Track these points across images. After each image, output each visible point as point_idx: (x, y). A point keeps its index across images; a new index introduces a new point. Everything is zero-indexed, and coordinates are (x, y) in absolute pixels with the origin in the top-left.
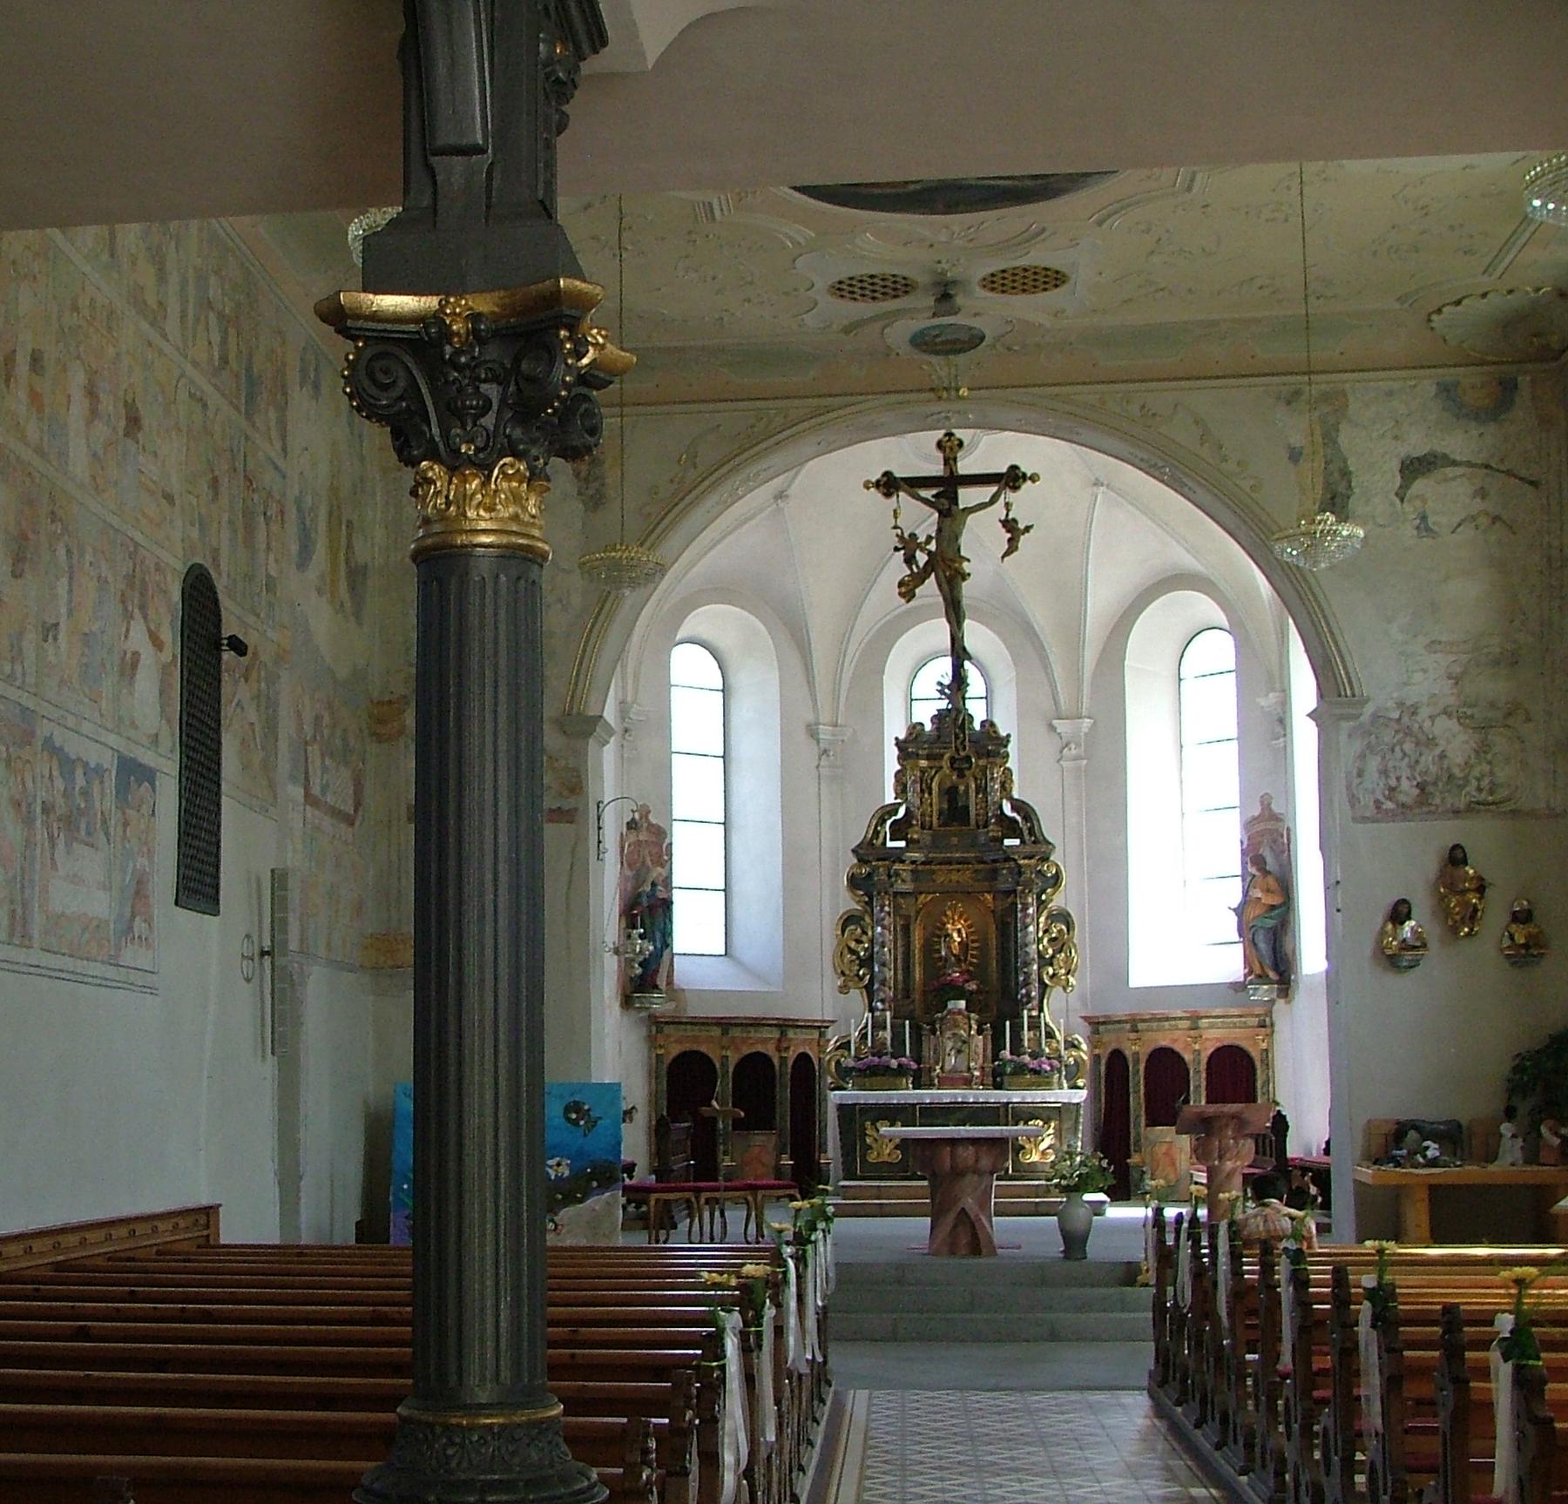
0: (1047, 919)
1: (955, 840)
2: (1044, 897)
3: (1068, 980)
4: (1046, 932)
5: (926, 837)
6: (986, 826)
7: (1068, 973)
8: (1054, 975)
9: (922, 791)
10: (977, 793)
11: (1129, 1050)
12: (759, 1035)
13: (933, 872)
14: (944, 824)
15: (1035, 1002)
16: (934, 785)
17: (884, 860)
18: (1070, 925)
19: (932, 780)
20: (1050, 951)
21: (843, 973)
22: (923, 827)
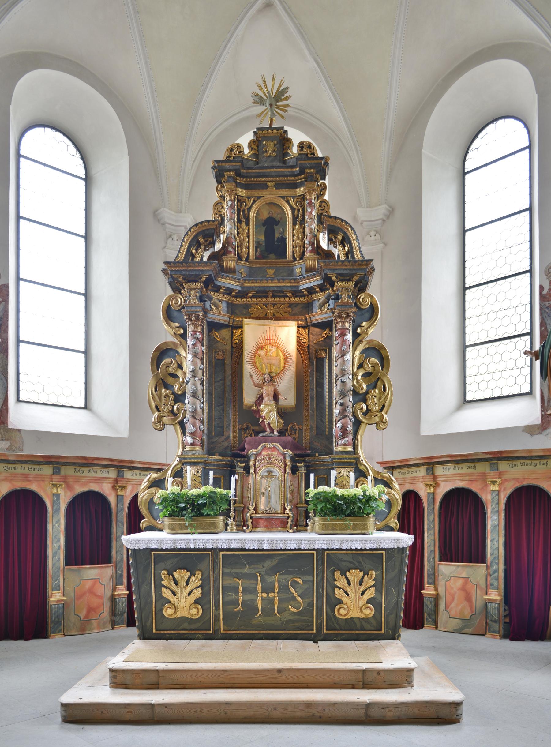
0: (361, 353)
1: (271, 272)
2: (359, 330)
3: (382, 416)
4: (361, 366)
5: (242, 267)
6: (302, 257)
7: (381, 410)
8: (368, 410)
9: (239, 221)
10: (294, 224)
11: (423, 492)
12: (94, 475)
13: (247, 306)
14: (260, 256)
15: (351, 437)
16: (252, 215)
17: (196, 281)
18: (384, 360)
19: (249, 209)
20: (364, 386)
21: (158, 409)
22: (240, 258)
